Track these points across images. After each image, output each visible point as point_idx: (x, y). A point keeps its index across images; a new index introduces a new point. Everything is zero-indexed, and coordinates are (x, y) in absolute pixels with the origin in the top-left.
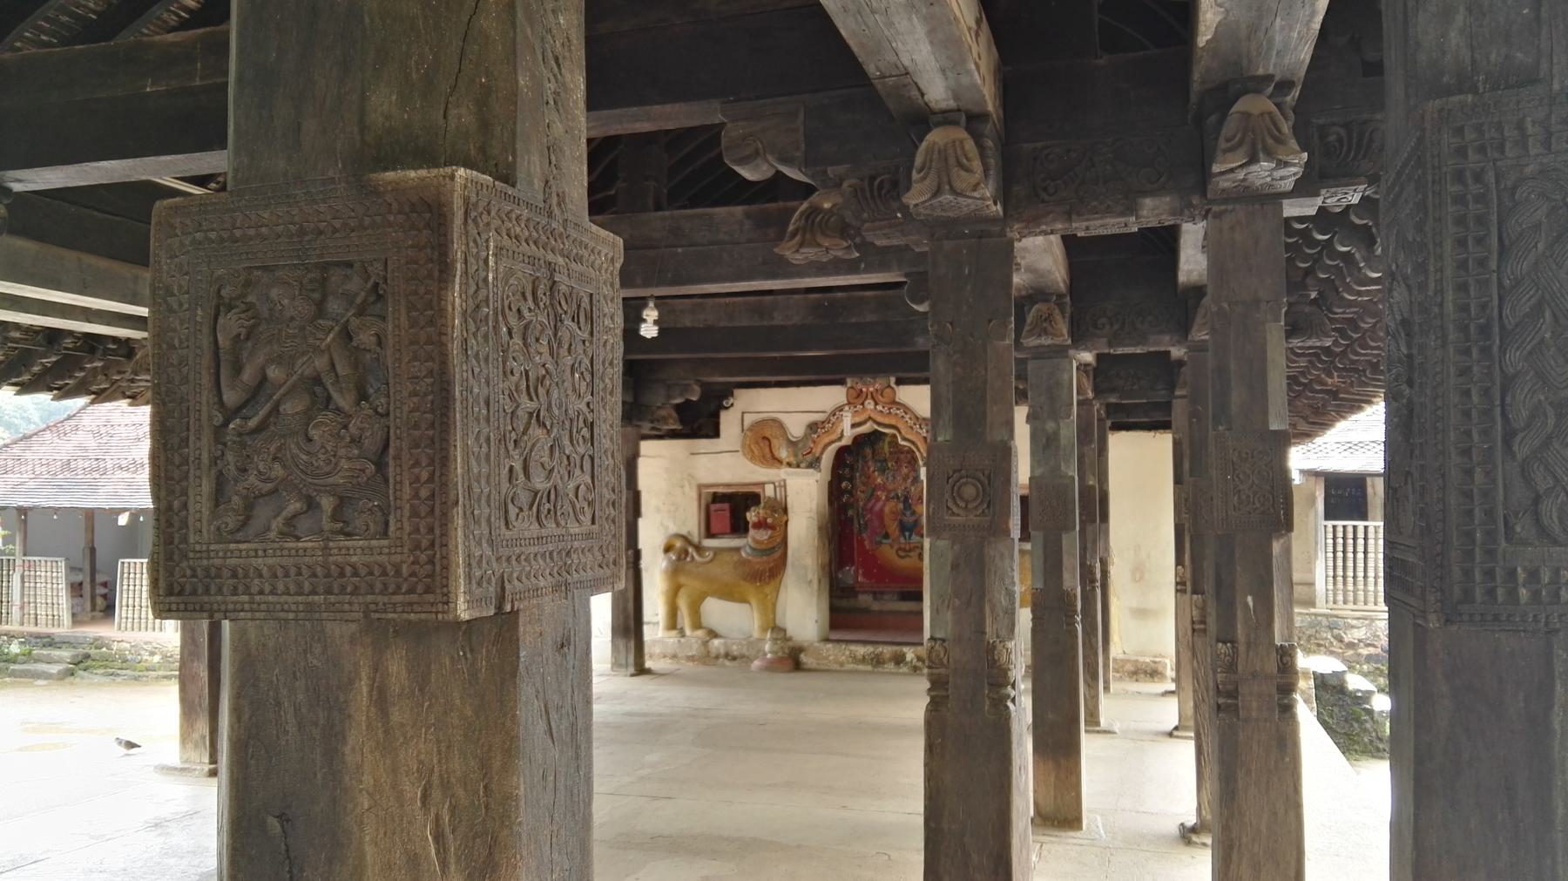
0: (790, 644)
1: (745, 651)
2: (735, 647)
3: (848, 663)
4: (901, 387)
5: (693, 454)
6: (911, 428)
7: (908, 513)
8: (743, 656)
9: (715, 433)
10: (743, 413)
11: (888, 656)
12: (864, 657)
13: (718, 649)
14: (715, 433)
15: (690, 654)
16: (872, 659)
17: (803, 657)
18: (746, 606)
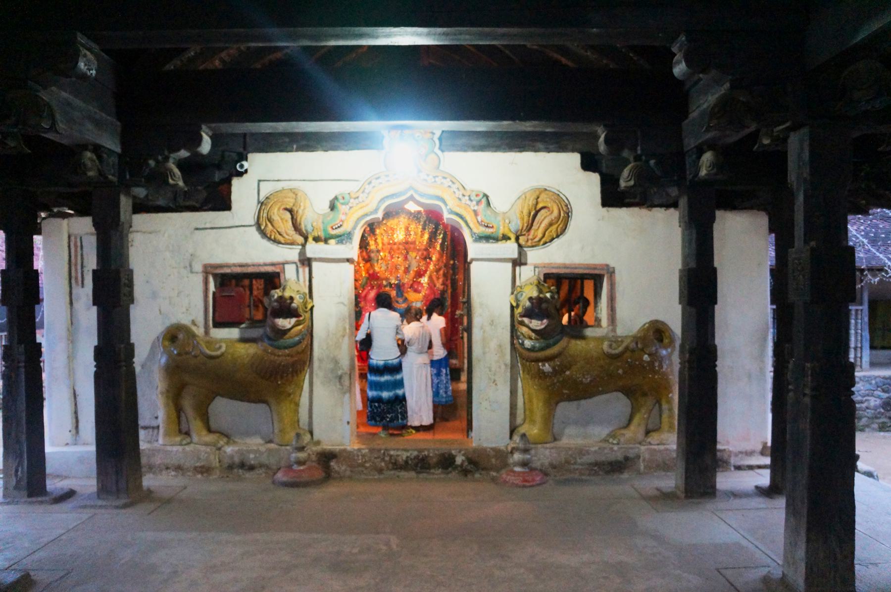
0: (318, 449)
1: (264, 459)
2: (252, 456)
3: (388, 469)
4: (446, 154)
5: (197, 229)
6: (460, 199)
7: (400, 300)
8: (261, 466)
9: (225, 205)
10: (260, 181)
11: (435, 460)
12: (406, 462)
13: (232, 457)
14: (223, 203)
15: (198, 464)
16: (416, 465)
17: (333, 464)
18: (263, 406)
